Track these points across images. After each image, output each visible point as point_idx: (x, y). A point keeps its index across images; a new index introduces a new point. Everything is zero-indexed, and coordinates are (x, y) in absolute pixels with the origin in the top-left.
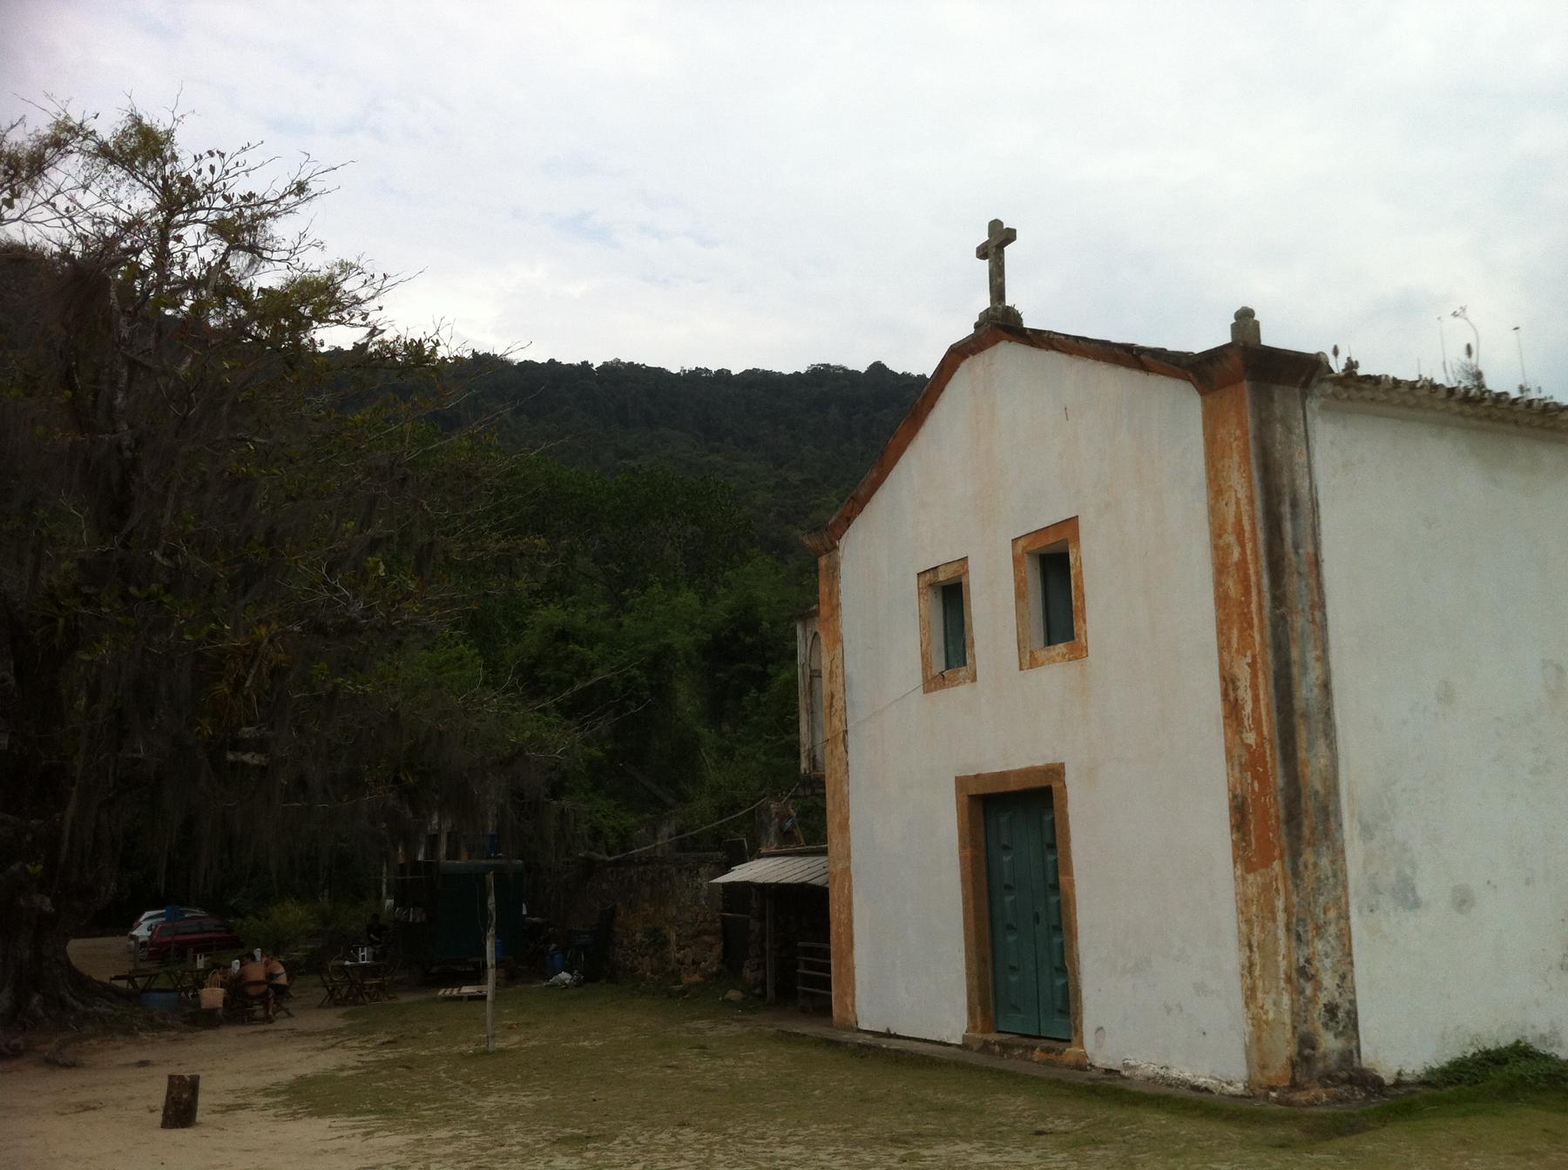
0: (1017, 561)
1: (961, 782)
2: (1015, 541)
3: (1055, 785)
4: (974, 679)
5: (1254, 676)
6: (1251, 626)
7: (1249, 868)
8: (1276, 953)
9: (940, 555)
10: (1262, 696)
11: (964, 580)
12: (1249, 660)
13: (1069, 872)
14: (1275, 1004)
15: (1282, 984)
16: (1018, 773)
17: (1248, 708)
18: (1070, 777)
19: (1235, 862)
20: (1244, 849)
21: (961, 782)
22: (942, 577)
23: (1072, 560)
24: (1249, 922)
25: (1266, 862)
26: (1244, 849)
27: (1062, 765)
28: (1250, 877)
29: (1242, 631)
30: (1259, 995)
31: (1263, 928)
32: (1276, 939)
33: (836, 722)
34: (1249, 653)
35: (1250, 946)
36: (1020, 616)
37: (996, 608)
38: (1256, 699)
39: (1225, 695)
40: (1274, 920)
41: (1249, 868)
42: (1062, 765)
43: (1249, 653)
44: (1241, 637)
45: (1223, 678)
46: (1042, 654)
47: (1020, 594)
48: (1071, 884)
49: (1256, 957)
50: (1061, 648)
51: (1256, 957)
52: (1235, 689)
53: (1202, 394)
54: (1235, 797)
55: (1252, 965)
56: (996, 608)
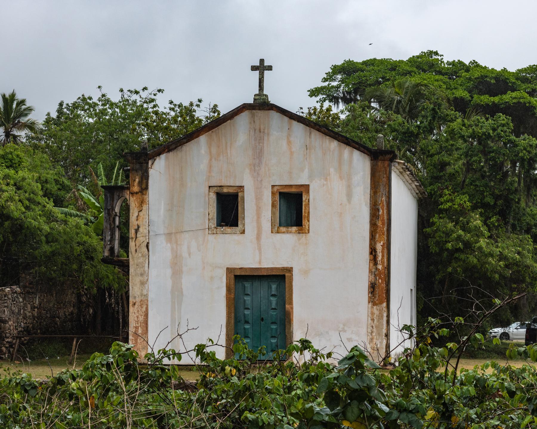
0: (273, 193)
1: (229, 270)
2: (273, 186)
3: (286, 275)
4: (243, 232)
5: (383, 249)
6: (383, 234)
7: (374, 304)
8: (383, 328)
9: (228, 181)
10: (385, 255)
11: (240, 194)
12: (382, 244)
13: (291, 303)
14: (380, 342)
15: (384, 337)
16: (267, 269)
17: (380, 258)
18: (295, 272)
19: (369, 302)
20: (373, 299)
21: (229, 270)
22: (225, 190)
23: (304, 199)
24: (373, 320)
25: (381, 303)
26: (373, 299)
27: (292, 268)
28: (375, 307)
29: (380, 235)
30: (375, 340)
31: (378, 321)
32: (383, 325)
33: (140, 239)
34: (382, 242)
35: (372, 327)
36: (273, 213)
37: (258, 208)
38: (383, 256)
39: (371, 253)
40: (383, 319)
41: (374, 304)
42: (292, 268)
43: (382, 242)
44: (379, 237)
45: (371, 248)
46: (283, 229)
47: (273, 205)
48: (292, 308)
49: (375, 330)
50: (294, 229)
51: (375, 330)
52: (376, 252)
53: (371, 160)
54: (371, 284)
55: (372, 332)
56: (258, 208)
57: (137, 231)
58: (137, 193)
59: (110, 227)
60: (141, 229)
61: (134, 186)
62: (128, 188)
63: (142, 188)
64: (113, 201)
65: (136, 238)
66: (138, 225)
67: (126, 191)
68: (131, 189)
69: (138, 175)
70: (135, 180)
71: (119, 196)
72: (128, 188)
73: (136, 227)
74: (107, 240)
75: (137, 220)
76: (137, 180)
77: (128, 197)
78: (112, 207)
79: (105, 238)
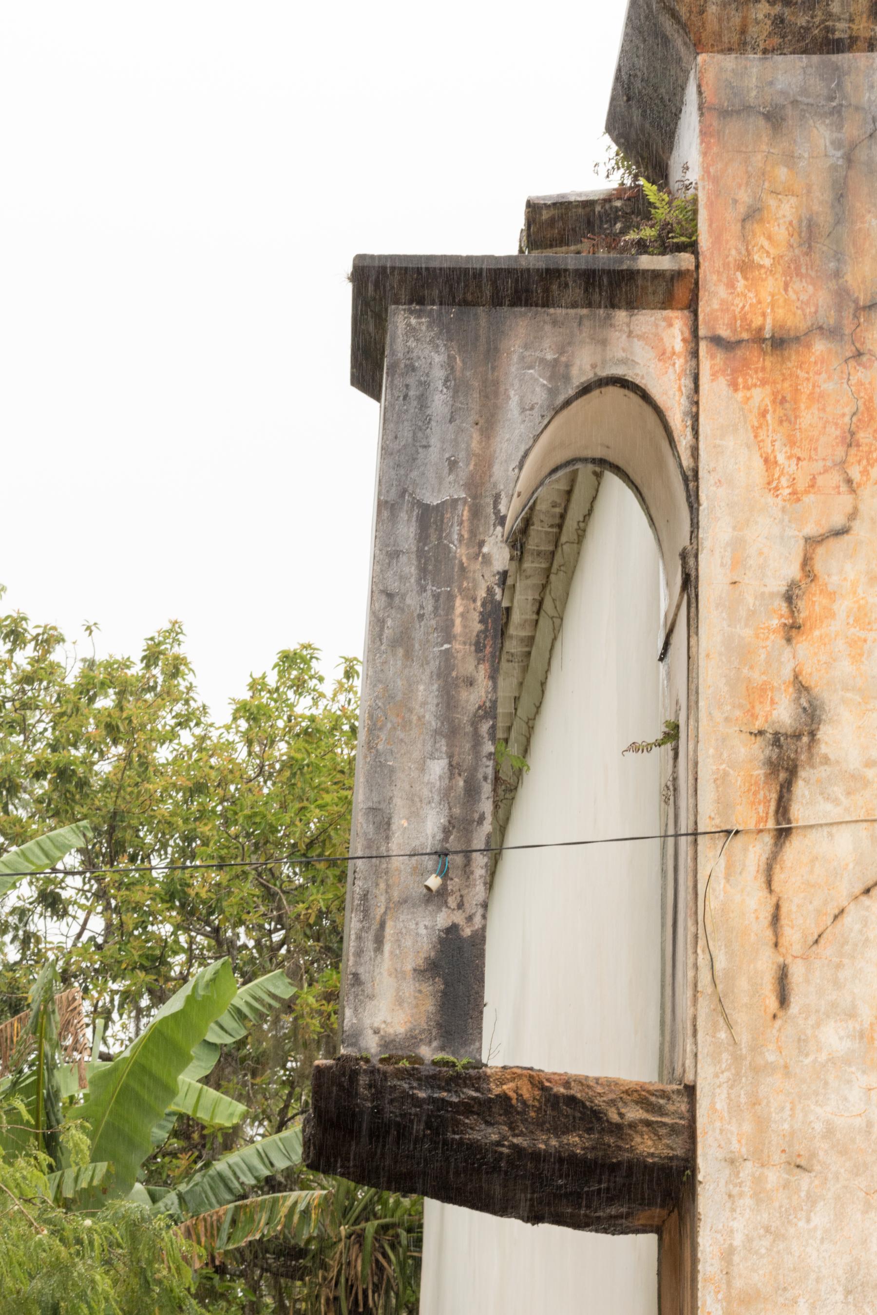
57: (787, 759)
58: (779, 343)
59: (449, 701)
60: (840, 739)
61: (746, 267)
62: (680, 292)
63: (842, 295)
64: (488, 424)
65: (783, 834)
66: (801, 687)
67: (647, 320)
68: (710, 303)
69: (790, 159)
70: (753, 215)
71: (558, 371)
72: (680, 292)
73: (783, 713)
74: (398, 843)
75: (792, 630)
76: (784, 212)
77: (668, 388)
78: (477, 486)
79: (382, 822)
